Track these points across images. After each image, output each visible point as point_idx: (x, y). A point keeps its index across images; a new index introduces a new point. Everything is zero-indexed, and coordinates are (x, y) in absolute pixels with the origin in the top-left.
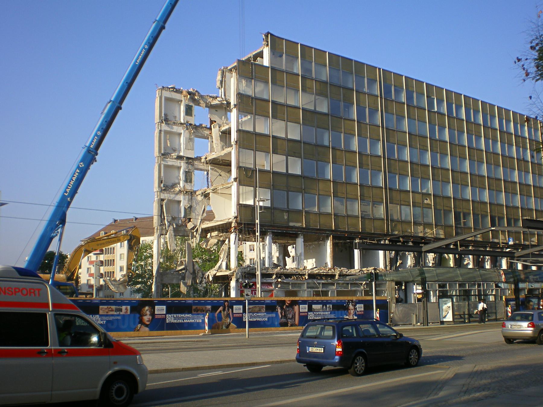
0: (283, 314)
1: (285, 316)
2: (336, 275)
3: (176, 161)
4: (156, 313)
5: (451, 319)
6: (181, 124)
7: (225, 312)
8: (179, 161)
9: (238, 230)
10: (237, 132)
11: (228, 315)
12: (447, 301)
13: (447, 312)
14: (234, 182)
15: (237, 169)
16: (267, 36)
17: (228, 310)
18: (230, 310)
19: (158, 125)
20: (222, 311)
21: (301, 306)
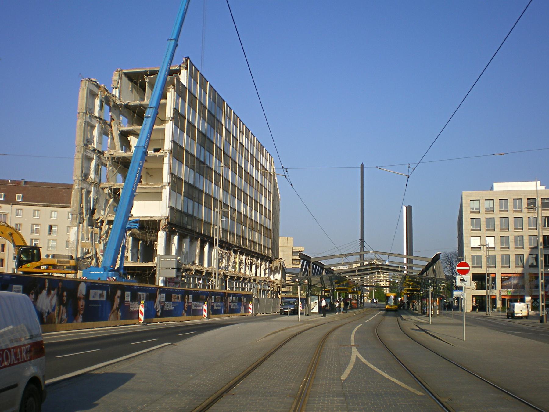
2: (203, 272)
3: (91, 152)
4: (189, 301)
5: (317, 311)
6: (96, 117)
8: (93, 153)
9: (168, 228)
10: (172, 143)
12: (315, 298)
13: (314, 306)
14: (166, 187)
15: (170, 175)
16: (187, 61)
19: (83, 115)
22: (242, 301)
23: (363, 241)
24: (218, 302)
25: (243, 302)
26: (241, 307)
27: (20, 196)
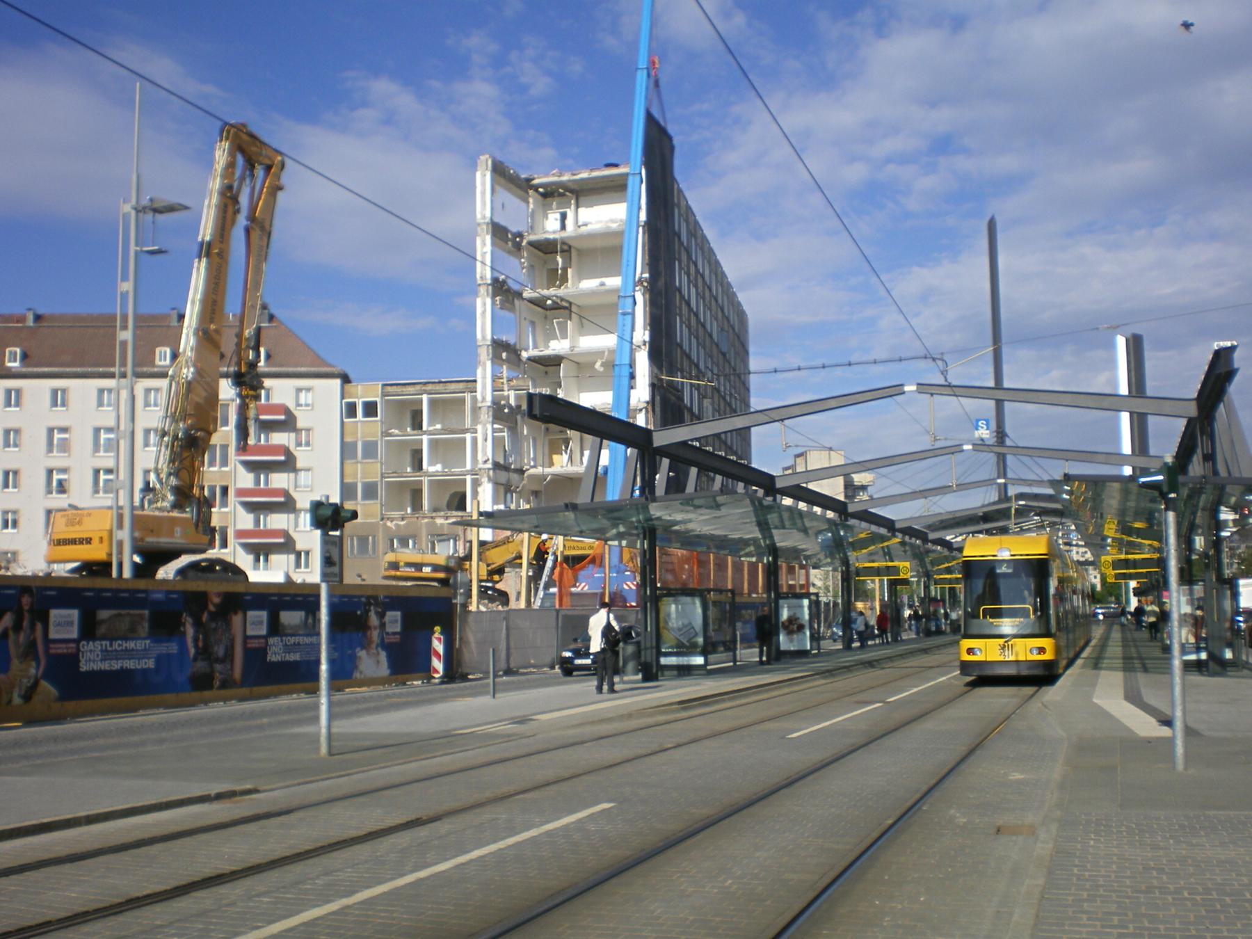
0: (201, 644)
1: (205, 652)
7: (22, 637)
11: (30, 651)
17: (33, 627)
18: (39, 627)
20: (11, 633)
21: (251, 614)
22: (363, 626)
23: (1002, 438)
24: (126, 639)
25: (375, 635)
26: (362, 654)
27: (16, 353)
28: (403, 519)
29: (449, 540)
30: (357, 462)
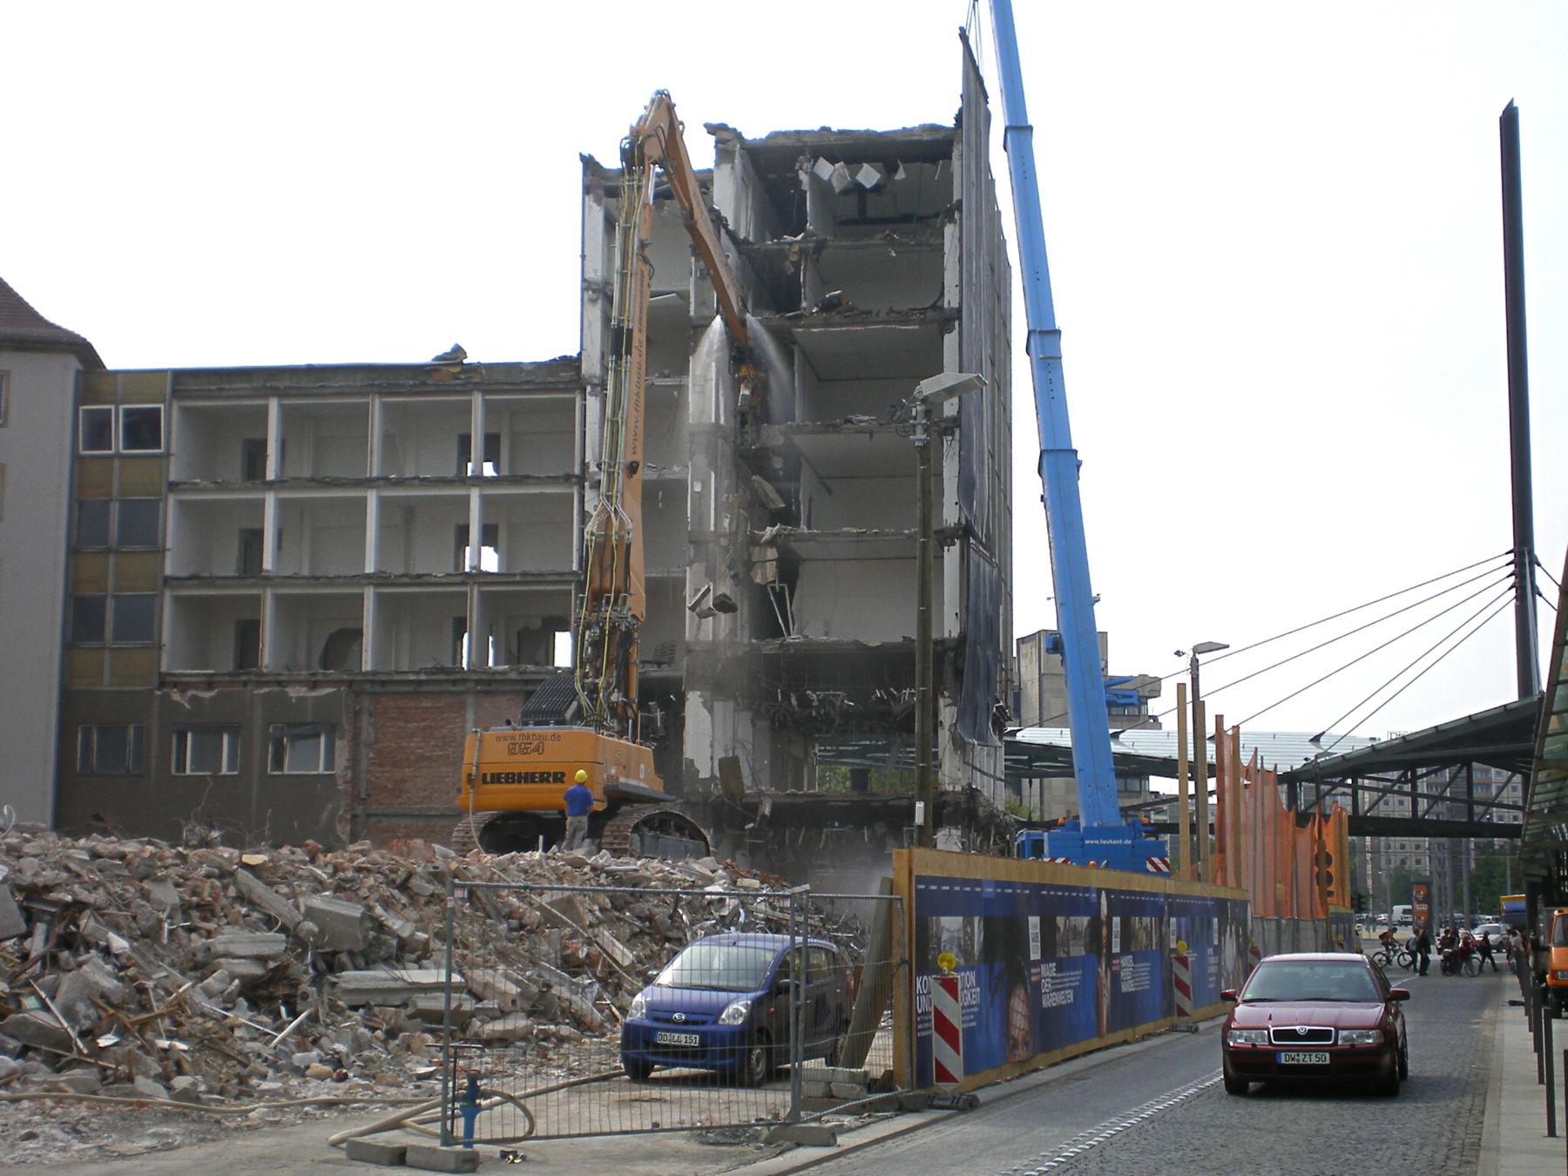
28: (210, 686)
29: (318, 736)
30: (108, 551)
